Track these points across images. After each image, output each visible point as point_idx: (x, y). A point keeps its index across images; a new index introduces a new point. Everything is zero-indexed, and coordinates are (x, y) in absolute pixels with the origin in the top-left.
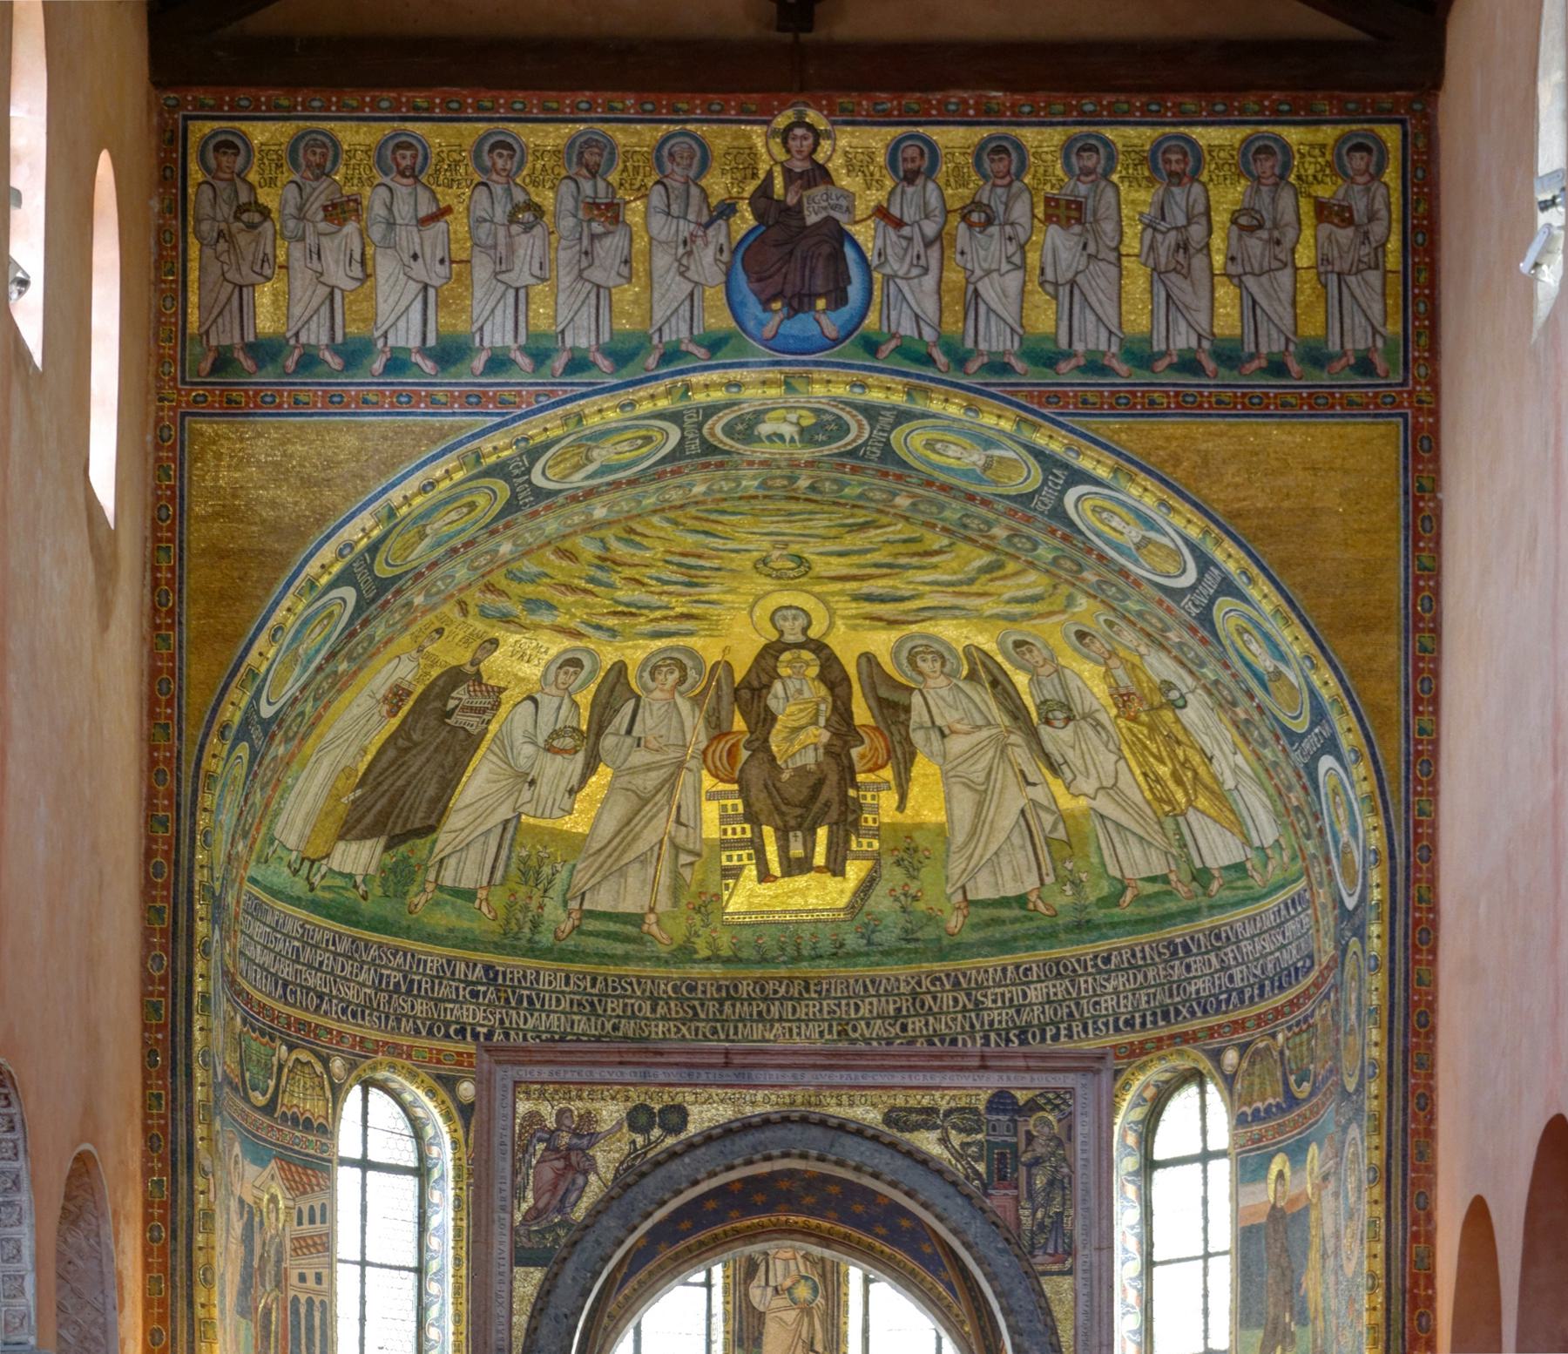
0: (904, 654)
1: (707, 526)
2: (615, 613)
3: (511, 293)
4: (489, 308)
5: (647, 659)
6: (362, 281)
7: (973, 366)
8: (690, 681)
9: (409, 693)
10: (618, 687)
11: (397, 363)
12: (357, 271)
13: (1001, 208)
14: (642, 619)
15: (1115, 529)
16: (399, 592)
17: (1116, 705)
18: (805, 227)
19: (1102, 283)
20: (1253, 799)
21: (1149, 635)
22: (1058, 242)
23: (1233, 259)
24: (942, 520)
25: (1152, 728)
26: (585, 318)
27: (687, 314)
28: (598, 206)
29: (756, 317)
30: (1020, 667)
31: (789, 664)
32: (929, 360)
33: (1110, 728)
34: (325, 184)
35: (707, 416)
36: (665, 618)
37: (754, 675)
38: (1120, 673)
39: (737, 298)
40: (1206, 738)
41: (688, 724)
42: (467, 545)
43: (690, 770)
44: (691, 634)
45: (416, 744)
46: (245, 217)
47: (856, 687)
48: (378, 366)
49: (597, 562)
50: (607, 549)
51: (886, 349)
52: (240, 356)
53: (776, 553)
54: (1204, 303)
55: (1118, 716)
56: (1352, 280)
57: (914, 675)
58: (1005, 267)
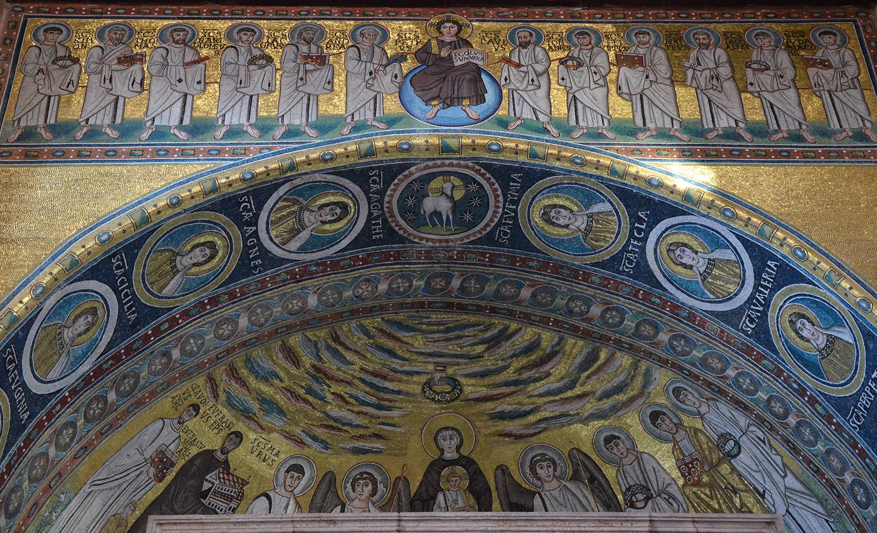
0: (528, 463)
1: (390, 344)
2: (327, 427)
3: (247, 98)
4: (230, 105)
6: (140, 93)
7: (576, 134)
8: (379, 493)
9: (173, 465)
11: (159, 134)
12: (137, 87)
13: (588, 60)
15: (685, 266)
16: (157, 331)
17: (683, 475)
18: (454, 66)
19: (663, 94)
20: (804, 513)
21: (709, 384)
22: (628, 75)
23: (751, 84)
24: (553, 311)
25: (712, 486)
26: (301, 109)
27: (372, 107)
28: (311, 57)
29: (420, 108)
30: (610, 462)
31: (448, 481)
32: (546, 131)
33: (680, 497)
34: (121, 47)
35: (387, 184)
36: (362, 437)
37: (423, 489)
38: (685, 443)
39: (406, 99)
40: (758, 476)
42: (214, 301)
44: (379, 452)
46: (60, 63)
47: (494, 494)
48: (145, 135)
49: (312, 371)
50: (321, 359)
51: (513, 125)
52: (43, 132)
53: (438, 376)
54: (736, 104)
55: (683, 486)
56: (840, 94)
57: (535, 481)
58: (593, 86)
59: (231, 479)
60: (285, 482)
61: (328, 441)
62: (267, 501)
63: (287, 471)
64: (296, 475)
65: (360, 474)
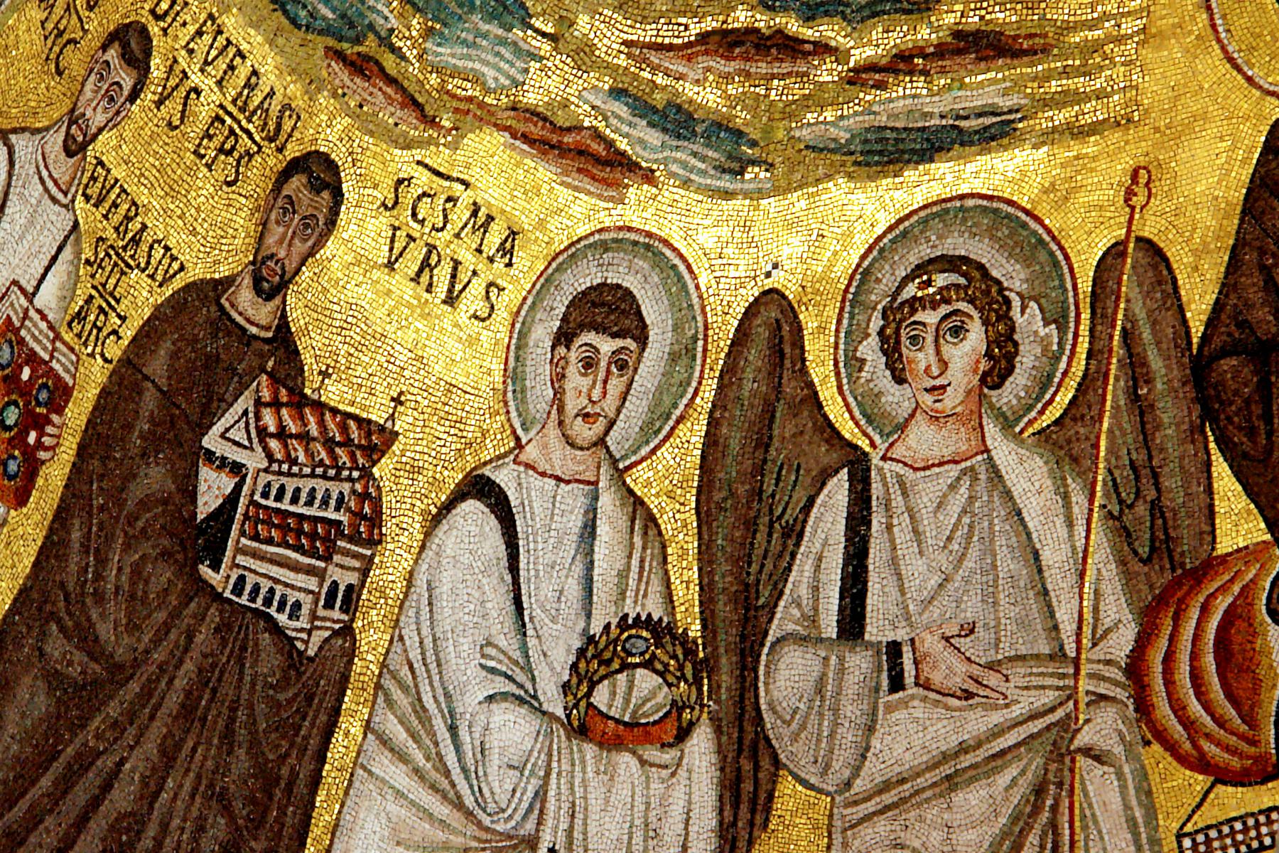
5: (863, 275)
8: (1027, 359)
9: (61, 394)
10: (783, 427)
14: (827, 72)
41: (1055, 556)
43: (1100, 758)
45: (118, 673)
59: (314, 430)
60: (559, 395)
61: (741, 117)
62: (493, 522)
63: (564, 337)
64: (607, 346)
65: (920, 269)
